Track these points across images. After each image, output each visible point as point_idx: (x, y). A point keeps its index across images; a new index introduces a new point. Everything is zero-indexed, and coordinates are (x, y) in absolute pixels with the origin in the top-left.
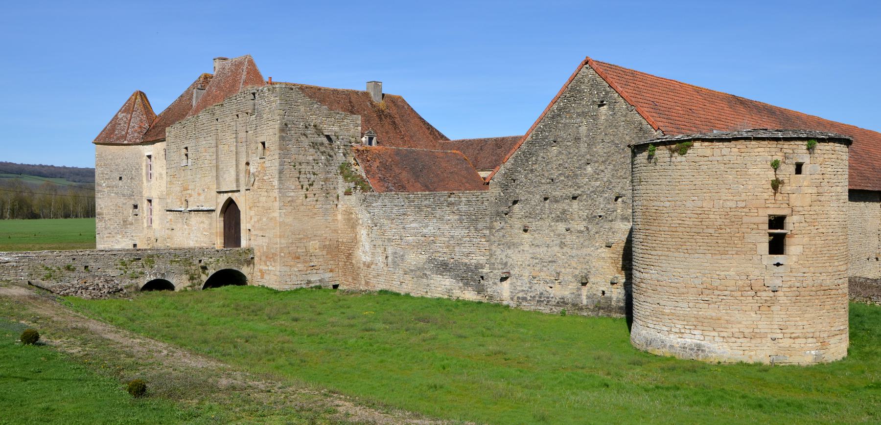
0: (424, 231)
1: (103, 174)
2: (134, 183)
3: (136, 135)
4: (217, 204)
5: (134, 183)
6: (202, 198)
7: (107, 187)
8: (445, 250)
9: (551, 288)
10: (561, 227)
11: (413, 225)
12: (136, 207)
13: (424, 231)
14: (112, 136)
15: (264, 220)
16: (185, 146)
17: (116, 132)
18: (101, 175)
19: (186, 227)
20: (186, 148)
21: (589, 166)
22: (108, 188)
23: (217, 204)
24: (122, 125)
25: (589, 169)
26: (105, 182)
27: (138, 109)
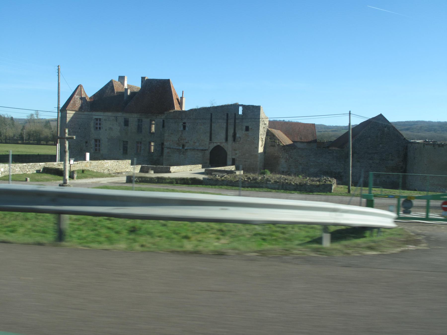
0: (318, 161)
1: (70, 125)
2: (86, 131)
3: (87, 107)
4: (209, 147)
5: (86, 131)
6: (197, 144)
7: (73, 132)
8: (326, 168)
9: (366, 179)
10: (371, 162)
11: (313, 159)
12: (86, 142)
13: (318, 161)
14: (75, 107)
15: (247, 155)
16: (184, 122)
17: (77, 105)
18: (70, 126)
19: (182, 155)
20: (184, 123)
21: (381, 145)
22: (73, 133)
23: (209, 147)
24: (78, 102)
25: (381, 146)
26: (71, 130)
27: (84, 94)
